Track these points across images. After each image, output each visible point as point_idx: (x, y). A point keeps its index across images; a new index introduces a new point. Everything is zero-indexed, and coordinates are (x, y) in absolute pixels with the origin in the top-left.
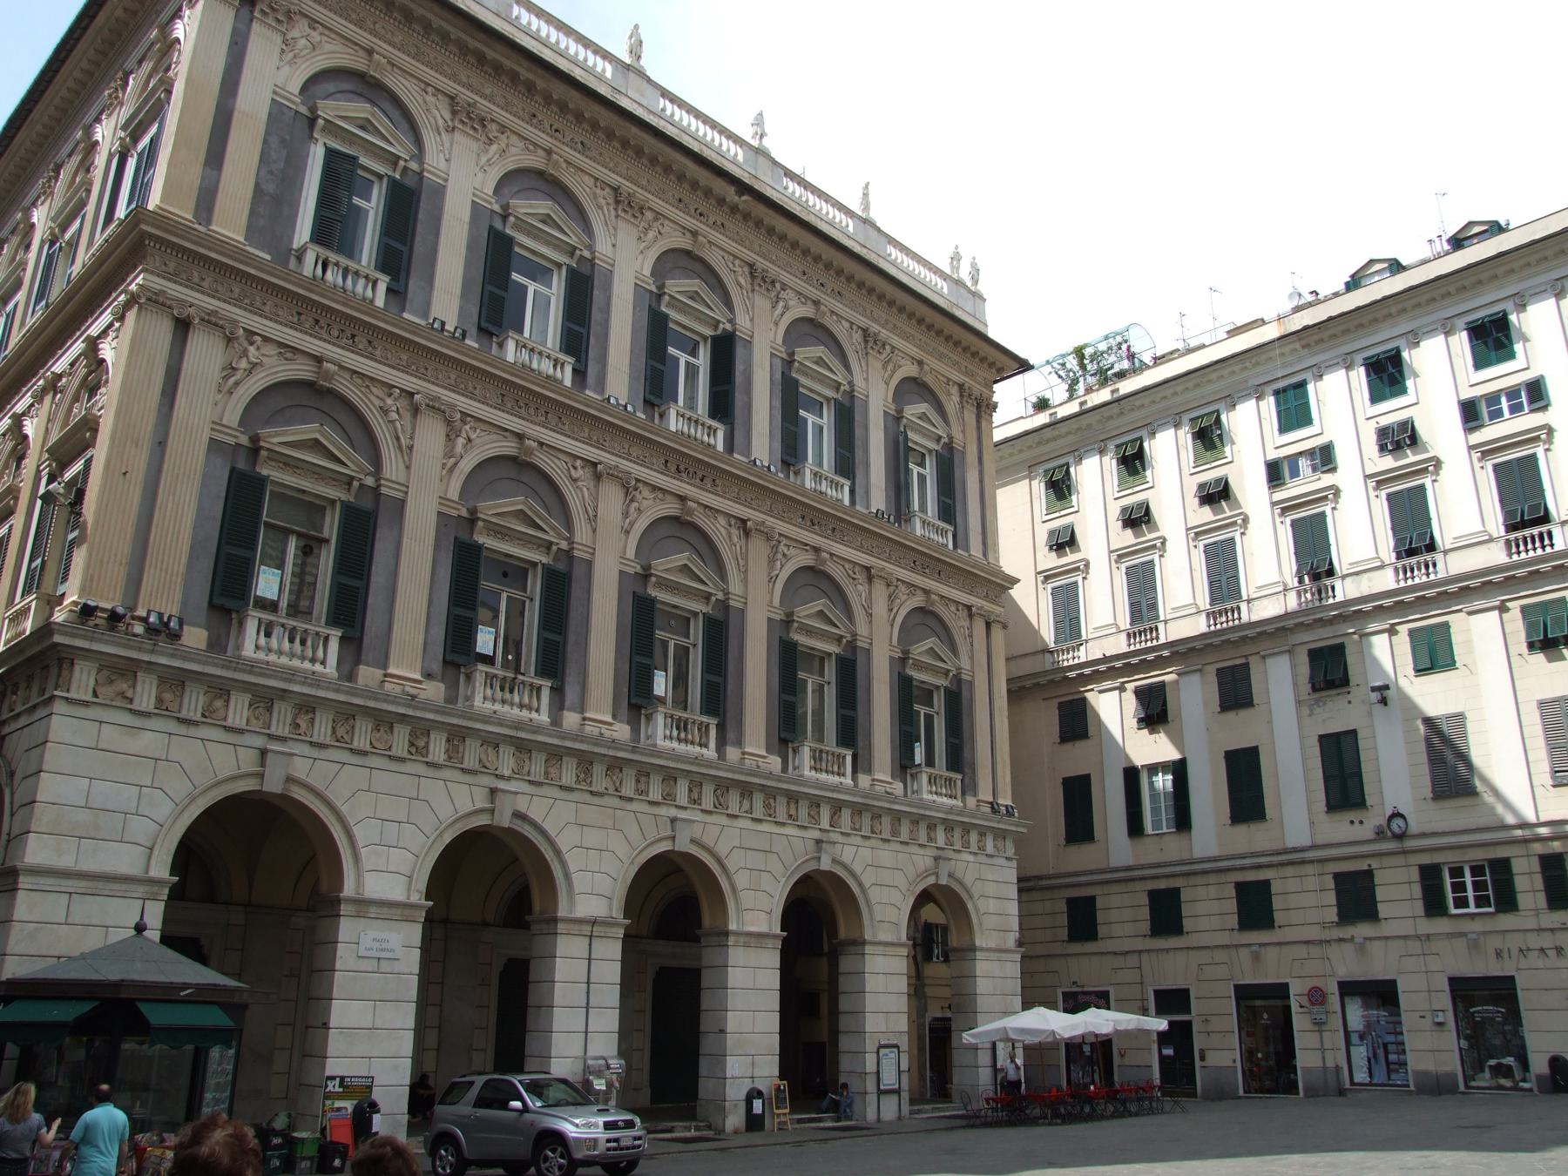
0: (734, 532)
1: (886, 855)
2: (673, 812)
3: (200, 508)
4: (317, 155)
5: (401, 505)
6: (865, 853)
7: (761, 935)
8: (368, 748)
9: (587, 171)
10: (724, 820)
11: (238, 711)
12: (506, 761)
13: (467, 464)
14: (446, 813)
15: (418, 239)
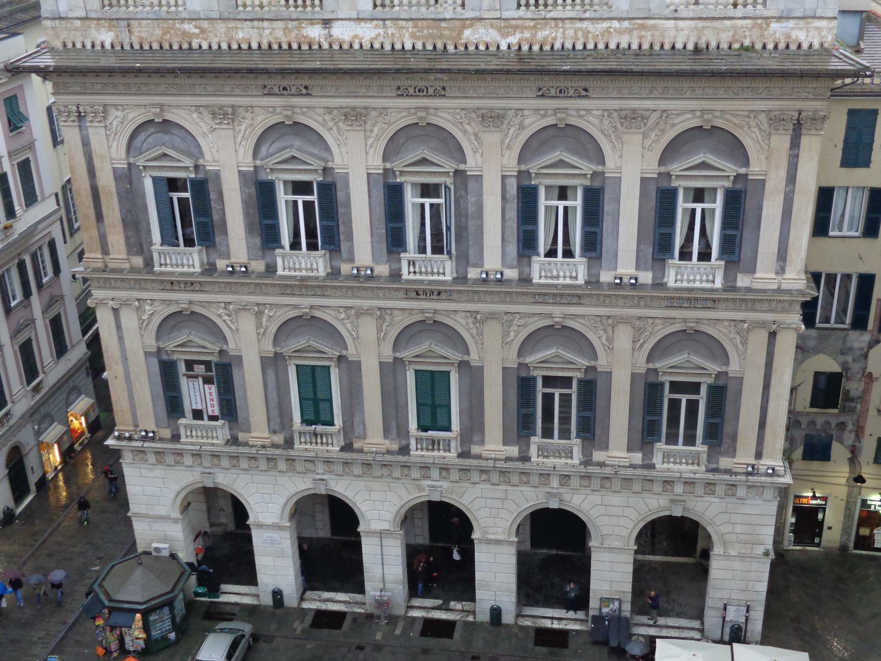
0: (470, 320)
1: (615, 499)
2: (429, 483)
4: (148, 184)
5: (240, 358)
6: (596, 498)
7: (498, 542)
8: (247, 467)
9: (315, 110)
10: (469, 485)
11: (188, 460)
12: (320, 468)
13: (273, 329)
14: (292, 490)
15: (214, 211)
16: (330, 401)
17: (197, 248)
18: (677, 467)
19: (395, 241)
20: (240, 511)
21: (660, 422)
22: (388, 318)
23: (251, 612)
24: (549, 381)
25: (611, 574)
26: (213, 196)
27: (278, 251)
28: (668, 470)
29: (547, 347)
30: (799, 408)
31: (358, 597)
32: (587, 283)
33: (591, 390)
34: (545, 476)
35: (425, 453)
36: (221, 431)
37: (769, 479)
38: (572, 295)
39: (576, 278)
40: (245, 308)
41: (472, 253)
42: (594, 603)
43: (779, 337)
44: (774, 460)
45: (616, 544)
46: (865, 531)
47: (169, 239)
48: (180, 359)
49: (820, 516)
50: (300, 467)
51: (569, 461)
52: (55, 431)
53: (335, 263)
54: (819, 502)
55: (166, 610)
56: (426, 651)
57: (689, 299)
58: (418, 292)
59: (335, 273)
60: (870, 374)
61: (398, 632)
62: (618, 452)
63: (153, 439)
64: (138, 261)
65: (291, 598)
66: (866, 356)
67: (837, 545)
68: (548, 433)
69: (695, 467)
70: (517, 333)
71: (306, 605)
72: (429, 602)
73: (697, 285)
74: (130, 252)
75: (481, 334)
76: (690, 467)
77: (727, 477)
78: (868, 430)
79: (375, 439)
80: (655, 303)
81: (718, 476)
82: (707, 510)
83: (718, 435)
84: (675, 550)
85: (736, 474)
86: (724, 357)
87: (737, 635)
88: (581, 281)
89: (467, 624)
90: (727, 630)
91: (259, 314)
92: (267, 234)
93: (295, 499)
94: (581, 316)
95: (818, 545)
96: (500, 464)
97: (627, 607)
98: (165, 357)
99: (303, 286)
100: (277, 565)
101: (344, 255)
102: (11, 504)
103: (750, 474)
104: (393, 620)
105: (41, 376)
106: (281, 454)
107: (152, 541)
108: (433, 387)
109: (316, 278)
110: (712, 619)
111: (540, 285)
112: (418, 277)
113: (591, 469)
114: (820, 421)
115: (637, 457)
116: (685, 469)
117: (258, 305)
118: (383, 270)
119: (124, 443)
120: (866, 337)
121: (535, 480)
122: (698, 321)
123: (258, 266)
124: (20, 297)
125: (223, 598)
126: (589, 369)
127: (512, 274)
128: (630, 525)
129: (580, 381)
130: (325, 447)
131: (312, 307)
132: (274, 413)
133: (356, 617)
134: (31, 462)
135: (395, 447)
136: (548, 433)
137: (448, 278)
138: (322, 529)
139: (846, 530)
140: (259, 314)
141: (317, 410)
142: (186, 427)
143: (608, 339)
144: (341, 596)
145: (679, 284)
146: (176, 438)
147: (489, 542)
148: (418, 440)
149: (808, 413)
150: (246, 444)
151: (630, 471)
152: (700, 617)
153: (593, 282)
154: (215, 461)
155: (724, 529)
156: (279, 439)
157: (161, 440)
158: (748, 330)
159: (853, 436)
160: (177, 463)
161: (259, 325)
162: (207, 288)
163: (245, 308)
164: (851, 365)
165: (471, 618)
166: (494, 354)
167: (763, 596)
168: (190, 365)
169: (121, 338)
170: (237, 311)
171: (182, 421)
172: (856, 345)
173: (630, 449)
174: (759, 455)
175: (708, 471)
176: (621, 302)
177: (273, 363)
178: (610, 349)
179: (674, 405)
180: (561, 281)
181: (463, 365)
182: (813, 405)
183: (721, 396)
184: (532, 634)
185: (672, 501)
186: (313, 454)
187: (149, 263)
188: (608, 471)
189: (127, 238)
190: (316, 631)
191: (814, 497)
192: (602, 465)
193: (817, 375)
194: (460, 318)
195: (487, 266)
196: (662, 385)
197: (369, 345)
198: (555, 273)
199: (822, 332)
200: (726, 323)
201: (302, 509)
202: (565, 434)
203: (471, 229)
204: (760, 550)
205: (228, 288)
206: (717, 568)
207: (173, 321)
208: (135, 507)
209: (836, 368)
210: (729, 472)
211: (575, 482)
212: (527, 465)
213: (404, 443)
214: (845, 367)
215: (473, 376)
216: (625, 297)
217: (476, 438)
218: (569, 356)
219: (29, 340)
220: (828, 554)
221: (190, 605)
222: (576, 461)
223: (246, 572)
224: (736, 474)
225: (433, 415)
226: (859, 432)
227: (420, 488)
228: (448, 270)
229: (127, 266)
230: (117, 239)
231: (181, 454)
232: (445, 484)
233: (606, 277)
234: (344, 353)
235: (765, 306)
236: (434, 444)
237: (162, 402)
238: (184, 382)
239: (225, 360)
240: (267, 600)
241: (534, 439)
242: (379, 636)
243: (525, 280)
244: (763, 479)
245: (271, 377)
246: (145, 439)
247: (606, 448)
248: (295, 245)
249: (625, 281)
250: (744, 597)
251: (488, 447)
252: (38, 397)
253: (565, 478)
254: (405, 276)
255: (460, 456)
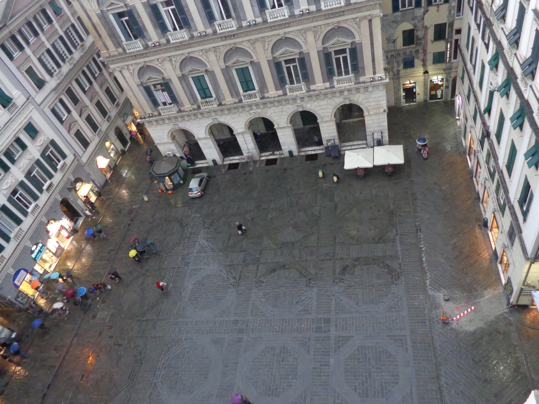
0: (249, 44)
1: (323, 103)
2: (253, 111)
3: (143, 96)
6: (316, 104)
7: (284, 128)
12: (213, 114)
13: (178, 65)
14: (207, 124)
16: (208, 88)
17: (139, 39)
18: (343, 85)
19: (210, 17)
20: (231, 130)
21: (333, 68)
22: (218, 50)
23: (207, 168)
24: (287, 62)
25: (328, 131)
26: (136, 16)
27: (168, 33)
28: (340, 87)
29: (282, 48)
30: (399, 48)
31: (242, 156)
32: (289, 17)
33: (303, 61)
34: (295, 99)
35: (248, 100)
36: (174, 109)
37: (380, 82)
38: (284, 24)
39: (285, 16)
40: (164, 59)
41: (241, 15)
42: (324, 142)
43: (373, 21)
44: (381, 74)
45: (327, 119)
46: (433, 93)
47: (128, 38)
48: (150, 84)
49: (414, 90)
50: (206, 115)
51: (302, 92)
52: (130, 118)
53: (191, 33)
54: (413, 85)
55: (176, 174)
56: (267, 171)
57: (332, 14)
58: (225, 37)
59: (192, 37)
60: (426, 26)
61: (257, 166)
62: (319, 84)
63: (152, 116)
64: (120, 50)
65: (219, 162)
66: (423, 19)
67: (423, 100)
68: (292, 82)
69: (350, 84)
70: (268, 45)
71: (225, 163)
72: (267, 154)
73: (334, 6)
74: (116, 47)
75: (254, 48)
76: (348, 84)
77: (363, 85)
78: (428, 51)
79: (229, 99)
80: (319, 19)
81: (359, 85)
82: (359, 99)
83: (357, 69)
84: (350, 117)
85: (367, 83)
86: (352, 35)
87: (380, 143)
88: (287, 16)
89: (281, 158)
90: (376, 142)
91: (171, 60)
92: (162, 28)
93: (208, 127)
94: (291, 31)
95: (415, 102)
96: (276, 99)
97: (337, 142)
98: (145, 85)
99: (181, 45)
100: (211, 152)
101: (193, 28)
102: (123, 148)
103: (372, 81)
104: (255, 162)
105: (118, 100)
106: (197, 113)
107: (166, 152)
108: (243, 73)
109: (185, 41)
110: (369, 139)
111: (271, 22)
112: (223, 31)
113: (311, 93)
114: (408, 51)
115: (328, 85)
116: (346, 85)
117: (169, 57)
118: (209, 31)
119: (143, 120)
120: (422, 10)
121: (291, 102)
122: (339, 22)
123: (163, 41)
124: (98, 72)
125: (197, 166)
126: (301, 53)
127: (259, 20)
128: (331, 111)
129: (298, 59)
130: (212, 106)
131: (189, 53)
132: (190, 97)
133: (243, 163)
134: (125, 131)
135: (237, 100)
136: (292, 82)
137: (235, 28)
138: (262, 129)
139: (425, 94)
140: (171, 60)
141: (205, 93)
142: (162, 109)
143: (304, 39)
144: (237, 157)
145: (327, 8)
146: (160, 114)
147: (281, 128)
148: (244, 96)
149: (403, 49)
150: (184, 111)
151: (326, 91)
152: (366, 139)
153: (292, 16)
154: (176, 120)
155: (367, 105)
156: (195, 107)
157: (155, 116)
158: (360, 21)
159: (423, 54)
160: (164, 123)
161: (172, 65)
162: (148, 55)
163: (164, 59)
164: (418, 24)
165: (282, 156)
166: (262, 56)
167: (386, 127)
168: (155, 86)
169: (127, 82)
170: (163, 61)
171: (160, 108)
172: (418, 14)
173: (324, 82)
174: (374, 73)
175: (355, 84)
176: (305, 22)
177: (183, 78)
178: (306, 42)
179: (338, 60)
180: (279, 18)
181: (252, 63)
182: (404, 45)
183: (355, 52)
184: (305, 158)
185: (344, 99)
186: (208, 110)
187: (124, 50)
188: (317, 92)
189: (113, 42)
190: (230, 171)
191: (410, 83)
192: (314, 90)
193: (404, 32)
194: (245, 44)
195: (249, 19)
196: (330, 53)
197: (214, 63)
198: (276, 15)
199: (403, 12)
200: (350, 20)
201: (252, 124)
202: (298, 81)
203: (238, 4)
204: (382, 110)
205: (156, 53)
206: (368, 120)
207: (142, 71)
208: (156, 142)
209: (411, 27)
210: (364, 82)
211: (306, 99)
212: (287, 97)
213: (240, 98)
214: (415, 26)
215: (257, 66)
216: (307, 19)
217: (265, 91)
218: (291, 50)
219: (108, 88)
220: (419, 104)
221: (185, 170)
222: (304, 91)
223: (202, 157)
224: (367, 83)
225: (248, 85)
226: (425, 52)
227: (250, 114)
228: (234, 25)
229: (117, 53)
230: (109, 43)
231: (164, 120)
232: (259, 110)
233: (297, 12)
234: (252, 60)
235: (365, 9)
236: (250, 96)
237: (150, 103)
238: (155, 93)
239: (166, 81)
240: (212, 164)
241: (287, 86)
242: (251, 169)
243: (265, 21)
244: (377, 82)
245: (184, 84)
246: (149, 117)
247: (315, 84)
248: (175, 29)
249: (304, 12)
250: (379, 129)
251: (271, 93)
252: (119, 108)
253: (302, 99)
254: (218, 32)
255: (261, 99)
